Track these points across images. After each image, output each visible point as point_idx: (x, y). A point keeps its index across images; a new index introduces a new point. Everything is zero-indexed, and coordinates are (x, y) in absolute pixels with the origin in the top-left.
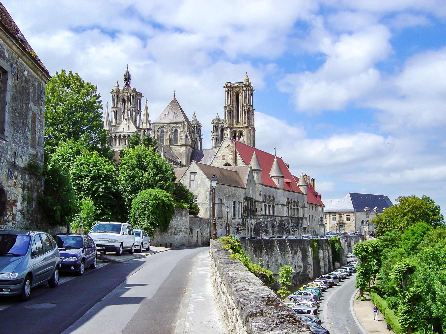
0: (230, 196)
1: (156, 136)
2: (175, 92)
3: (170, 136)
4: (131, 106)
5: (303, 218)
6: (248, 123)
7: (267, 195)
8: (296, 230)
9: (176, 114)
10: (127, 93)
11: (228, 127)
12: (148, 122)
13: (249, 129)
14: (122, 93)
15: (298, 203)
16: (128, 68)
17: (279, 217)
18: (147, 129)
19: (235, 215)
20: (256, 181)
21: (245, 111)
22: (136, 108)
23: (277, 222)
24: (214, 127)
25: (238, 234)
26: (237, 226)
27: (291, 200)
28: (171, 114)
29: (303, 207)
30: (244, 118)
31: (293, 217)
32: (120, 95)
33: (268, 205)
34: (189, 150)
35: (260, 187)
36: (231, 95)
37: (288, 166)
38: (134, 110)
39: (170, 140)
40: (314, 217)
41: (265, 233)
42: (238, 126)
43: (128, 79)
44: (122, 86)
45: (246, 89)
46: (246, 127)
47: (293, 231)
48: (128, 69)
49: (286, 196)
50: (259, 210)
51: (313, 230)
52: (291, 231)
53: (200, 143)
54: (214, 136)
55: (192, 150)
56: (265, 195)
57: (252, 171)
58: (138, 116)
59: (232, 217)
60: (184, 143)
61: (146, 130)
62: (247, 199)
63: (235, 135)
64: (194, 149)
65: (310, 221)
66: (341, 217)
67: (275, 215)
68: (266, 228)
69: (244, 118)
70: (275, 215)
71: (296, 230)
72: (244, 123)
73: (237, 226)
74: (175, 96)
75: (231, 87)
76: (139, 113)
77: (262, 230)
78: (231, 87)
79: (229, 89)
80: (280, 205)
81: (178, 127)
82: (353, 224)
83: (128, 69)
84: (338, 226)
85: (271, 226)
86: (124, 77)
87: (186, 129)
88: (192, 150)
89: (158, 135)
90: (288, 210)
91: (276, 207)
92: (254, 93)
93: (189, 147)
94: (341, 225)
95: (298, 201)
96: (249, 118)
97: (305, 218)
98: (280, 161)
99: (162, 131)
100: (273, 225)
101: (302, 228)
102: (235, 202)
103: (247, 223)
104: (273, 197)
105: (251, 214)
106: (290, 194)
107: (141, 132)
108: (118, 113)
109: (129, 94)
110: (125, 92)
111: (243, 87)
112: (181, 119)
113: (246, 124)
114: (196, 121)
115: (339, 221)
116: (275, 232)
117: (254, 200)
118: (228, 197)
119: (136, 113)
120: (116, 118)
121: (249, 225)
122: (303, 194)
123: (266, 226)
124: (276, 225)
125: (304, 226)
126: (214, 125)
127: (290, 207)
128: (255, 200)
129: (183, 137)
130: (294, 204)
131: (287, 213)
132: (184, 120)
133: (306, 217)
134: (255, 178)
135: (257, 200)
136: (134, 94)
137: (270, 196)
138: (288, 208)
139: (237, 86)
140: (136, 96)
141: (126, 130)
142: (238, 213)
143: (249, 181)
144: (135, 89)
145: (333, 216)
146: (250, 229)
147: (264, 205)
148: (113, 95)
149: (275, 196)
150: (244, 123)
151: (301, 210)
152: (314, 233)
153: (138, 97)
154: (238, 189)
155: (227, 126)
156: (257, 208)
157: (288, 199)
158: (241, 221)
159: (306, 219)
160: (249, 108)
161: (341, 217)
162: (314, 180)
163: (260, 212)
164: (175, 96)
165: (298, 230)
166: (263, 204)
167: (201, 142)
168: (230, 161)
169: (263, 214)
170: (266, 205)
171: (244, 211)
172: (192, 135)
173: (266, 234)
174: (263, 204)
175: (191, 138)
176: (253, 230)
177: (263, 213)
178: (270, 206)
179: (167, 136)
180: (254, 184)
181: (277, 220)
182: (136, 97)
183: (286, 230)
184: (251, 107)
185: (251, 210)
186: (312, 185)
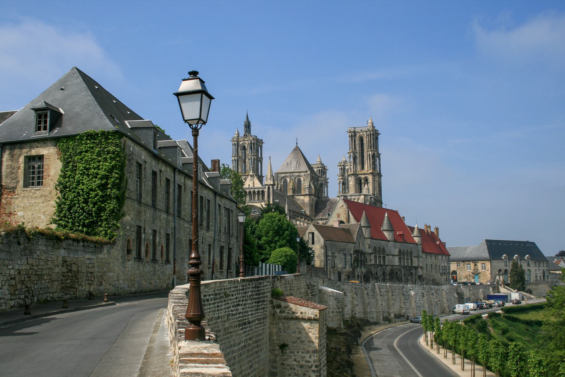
1: (279, 186)
2: (297, 139)
3: (293, 185)
4: (253, 154)
5: (418, 267)
6: (374, 169)
7: (377, 247)
8: (410, 278)
9: (298, 163)
10: (248, 141)
11: (352, 174)
12: (272, 179)
14: (243, 141)
15: (411, 253)
17: (390, 267)
18: (271, 185)
19: (346, 265)
20: (366, 236)
21: (369, 156)
22: (257, 155)
24: (341, 170)
27: (404, 250)
28: (294, 163)
29: (418, 257)
30: (369, 163)
31: (406, 266)
32: (241, 143)
33: (379, 256)
34: (313, 200)
35: (368, 241)
37: (404, 218)
39: (294, 190)
40: (434, 266)
41: (375, 280)
42: (363, 172)
43: (248, 126)
44: (242, 134)
45: (370, 133)
46: (371, 173)
47: (406, 279)
48: (247, 115)
49: (398, 247)
50: (368, 260)
51: (431, 278)
52: (403, 279)
53: (326, 188)
54: (341, 180)
55: (315, 199)
56: (375, 248)
57: (361, 227)
58: (260, 163)
59: (344, 267)
60: (307, 193)
61: (271, 187)
62: (356, 252)
63: (361, 181)
64: (318, 197)
65: (428, 270)
66: (476, 265)
67: (386, 264)
68: (376, 276)
69: (369, 163)
70: (386, 264)
71: (410, 278)
72: (369, 169)
74: (297, 143)
75: (355, 132)
76: (260, 161)
77: (372, 278)
78: (355, 132)
79: (353, 135)
80: (391, 255)
81: (301, 176)
82: (488, 273)
83: (247, 115)
84: (473, 275)
85: (381, 274)
86: (244, 124)
87: (309, 178)
88: (315, 199)
89: (281, 185)
90: (401, 260)
91: (387, 257)
93: (313, 197)
94: (476, 274)
96: (374, 163)
97: (420, 267)
98: (394, 214)
99: (285, 181)
100: (384, 274)
101: (417, 276)
102: (345, 254)
104: (384, 249)
105: (361, 264)
106: (403, 245)
107: (265, 188)
109: (249, 141)
110: (246, 139)
111: (367, 132)
112: (304, 168)
113: (371, 170)
114: (321, 164)
115: (473, 270)
118: (340, 251)
119: (257, 161)
120: (238, 167)
122: (417, 244)
125: (419, 274)
126: (340, 167)
127: (402, 257)
128: (365, 252)
129: (307, 187)
130: (407, 254)
131: (399, 262)
132: (307, 169)
133: (421, 265)
134: (364, 233)
135: (366, 252)
136: (255, 142)
137: (380, 248)
139: (361, 130)
140: (257, 143)
141: (251, 185)
142: (349, 264)
143: (359, 237)
144: (256, 137)
145: (482, 264)
146: (360, 277)
148: (234, 143)
149: (385, 248)
150: (369, 169)
151: (415, 260)
152: (433, 281)
153: (259, 144)
154: (348, 244)
155: (352, 173)
156: (366, 259)
158: (351, 270)
159: (422, 268)
160: (374, 154)
161: (476, 265)
162: (437, 229)
164: (297, 143)
165: (412, 277)
166: (373, 256)
167: (327, 187)
168: (343, 219)
169: (373, 263)
170: (376, 256)
171: (354, 262)
172: (316, 183)
174: (373, 256)
175: (315, 187)
176: (362, 278)
177: (373, 262)
178: (380, 256)
179: (290, 186)
180: (364, 239)
181: (388, 269)
182: (256, 144)
183: (398, 278)
184: (376, 153)
185: (361, 261)
186: (436, 233)
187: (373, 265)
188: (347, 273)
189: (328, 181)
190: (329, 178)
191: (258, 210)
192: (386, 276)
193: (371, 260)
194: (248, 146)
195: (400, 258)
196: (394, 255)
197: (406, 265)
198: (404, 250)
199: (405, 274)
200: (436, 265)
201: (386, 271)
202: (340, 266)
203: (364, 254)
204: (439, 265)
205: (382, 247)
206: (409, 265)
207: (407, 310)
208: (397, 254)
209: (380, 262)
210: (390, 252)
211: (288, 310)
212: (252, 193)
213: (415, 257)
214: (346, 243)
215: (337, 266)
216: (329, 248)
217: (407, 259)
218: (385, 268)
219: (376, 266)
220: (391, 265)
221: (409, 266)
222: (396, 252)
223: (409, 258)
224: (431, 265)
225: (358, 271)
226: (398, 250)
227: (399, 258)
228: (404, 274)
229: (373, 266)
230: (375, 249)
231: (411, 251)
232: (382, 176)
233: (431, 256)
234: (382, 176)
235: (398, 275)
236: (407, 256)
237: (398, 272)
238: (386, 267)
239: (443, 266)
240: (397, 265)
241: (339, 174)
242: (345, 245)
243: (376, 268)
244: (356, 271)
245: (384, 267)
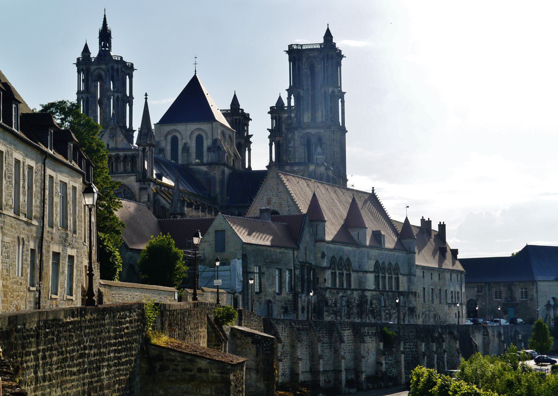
0: (272, 262)
2: (195, 64)
8: (394, 311)
13: (334, 131)
16: (105, 15)
17: (360, 292)
23: (356, 298)
25: (287, 315)
26: (286, 304)
27: (383, 263)
31: (388, 291)
33: (339, 273)
36: (299, 66)
38: (120, 97)
40: (437, 292)
41: (333, 316)
44: (94, 52)
47: (387, 314)
48: (105, 19)
49: (373, 257)
50: (321, 280)
52: (383, 313)
53: (247, 152)
56: (333, 257)
65: (426, 298)
67: (352, 287)
68: (335, 309)
70: (352, 287)
71: (394, 311)
73: (286, 304)
74: (195, 71)
77: (326, 311)
80: (361, 271)
83: (105, 19)
90: (379, 281)
91: (354, 275)
92: (343, 61)
95: (396, 264)
97: (412, 293)
101: (406, 308)
103: (301, 300)
104: (348, 259)
108: (90, 102)
116: (352, 314)
117: (313, 265)
121: (304, 302)
123: (336, 306)
124: (354, 304)
125: (411, 305)
127: (381, 275)
130: (390, 269)
131: (375, 284)
136: (119, 68)
138: (378, 276)
140: (123, 69)
144: (121, 58)
146: (306, 310)
147: (332, 272)
149: (351, 259)
152: (435, 318)
156: (318, 278)
157: (377, 262)
158: (290, 297)
163: (323, 284)
164: (195, 71)
165: (398, 311)
167: (250, 150)
169: (330, 286)
170: (335, 273)
173: (336, 317)
178: (343, 274)
183: (374, 313)
184: (336, 90)
187: (328, 288)
188: (283, 303)
189: (251, 139)
190: (252, 135)
191: (124, 190)
192: (352, 308)
193: (325, 279)
194: (106, 74)
195: (377, 278)
196: (367, 272)
197: (387, 289)
198: (383, 263)
199: (385, 304)
200: (440, 290)
201: (353, 300)
202: (270, 290)
203: (314, 270)
204: (446, 290)
205: (345, 258)
206: (394, 290)
207: (389, 368)
208: (372, 269)
209: (342, 284)
210: (360, 266)
211: (175, 365)
212: (114, 160)
213: (404, 275)
214: (282, 250)
215: (265, 291)
216: (252, 259)
217: (390, 278)
218: (350, 295)
219: (335, 291)
220: (360, 290)
221: (392, 292)
222: (370, 265)
223: (394, 276)
224: (432, 289)
225: (303, 300)
226: (373, 262)
227: (375, 276)
228: (383, 305)
229: (329, 290)
230: (333, 260)
231: (396, 264)
232: (347, 131)
233: (432, 274)
234: (347, 131)
235: (374, 306)
236: (390, 274)
237: (374, 301)
238: (353, 293)
239: (452, 292)
240: (373, 289)
241: (270, 128)
242: (280, 253)
243: (334, 294)
244: (299, 299)
245: (349, 292)
